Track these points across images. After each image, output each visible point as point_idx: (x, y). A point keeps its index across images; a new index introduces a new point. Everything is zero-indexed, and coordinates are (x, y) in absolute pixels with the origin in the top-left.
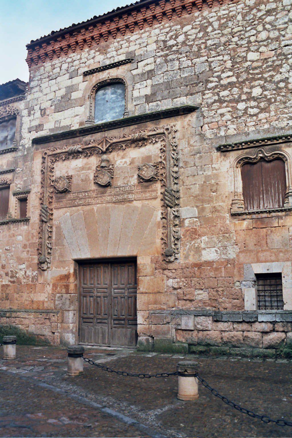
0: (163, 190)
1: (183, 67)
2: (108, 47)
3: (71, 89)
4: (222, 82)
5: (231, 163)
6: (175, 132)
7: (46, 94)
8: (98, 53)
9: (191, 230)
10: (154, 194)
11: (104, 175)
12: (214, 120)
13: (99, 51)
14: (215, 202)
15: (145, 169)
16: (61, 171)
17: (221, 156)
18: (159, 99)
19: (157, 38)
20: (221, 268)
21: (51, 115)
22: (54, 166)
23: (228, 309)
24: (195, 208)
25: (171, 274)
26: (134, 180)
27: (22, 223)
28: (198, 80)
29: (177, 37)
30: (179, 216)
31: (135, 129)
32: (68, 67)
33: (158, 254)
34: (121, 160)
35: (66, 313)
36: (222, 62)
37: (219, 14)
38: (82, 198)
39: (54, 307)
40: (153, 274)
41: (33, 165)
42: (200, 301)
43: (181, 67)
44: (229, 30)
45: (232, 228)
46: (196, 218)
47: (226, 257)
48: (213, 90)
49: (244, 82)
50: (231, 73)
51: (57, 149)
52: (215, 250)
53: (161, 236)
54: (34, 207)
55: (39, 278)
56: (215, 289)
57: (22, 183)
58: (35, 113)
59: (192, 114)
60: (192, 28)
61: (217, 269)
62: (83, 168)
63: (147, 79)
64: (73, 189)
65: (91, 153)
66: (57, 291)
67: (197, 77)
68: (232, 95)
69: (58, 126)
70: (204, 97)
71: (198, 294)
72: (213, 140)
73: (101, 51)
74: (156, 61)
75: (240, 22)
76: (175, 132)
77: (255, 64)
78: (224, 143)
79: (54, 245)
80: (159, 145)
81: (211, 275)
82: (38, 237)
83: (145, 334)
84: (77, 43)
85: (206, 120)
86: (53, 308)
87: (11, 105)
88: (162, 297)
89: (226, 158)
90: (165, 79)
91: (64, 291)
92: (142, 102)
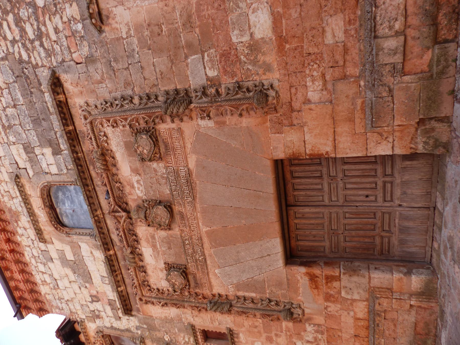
0: (168, 119)
1: (11, 102)
2: (10, 210)
3: (64, 261)
4: (18, 38)
7: (75, 294)
8: (19, 222)
9: (223, 63)
10: (176, 135)
11: (157, 215)
12: (65, 44)
13: (16, 222)
14: (176, 25)
15: (140, 149)
16: (161, 279)
17: (108, 25)
18: (54, 134)
21: (97, 288)
24: (189, 60)
25: (299, 95)
27: (236, 340)
28: (21, 76)
30: (204, 88)
31: (94, 168)
32: (41, 263)
33: (266, 121)
34: (136, 189)
38: (193, 249)
39: (364, 301)
41: (158, 318)
42: (346, 32)
43: (12, 103)
46: (203, 59)
48: (29, 50)
52: (253, 13)
53: (235, 118)
54: (212, 321)
55: (317, 322)
57: (182, 335)
58: (97, 310)
59: (63, 81)
62: (154, 247)
63: (35, 153)
64: (182, 261)
65: (133, 235)
66: (336, 296)
67: (18, 79)
68: (29, 18)
71: (334, 36)
72: (91, 42)
74: (13, 142)
76: (88, 105)
79: (264, 296)
80: (109, 130)
81: (296, 15)
82: (255, 320)
83: (412, 139)
86: (365, 303)
87: (93, 340)
88: (340, 107)
89: (112, 15)
90: (29, 127)
91: (336, 284)
92: (62, 159)
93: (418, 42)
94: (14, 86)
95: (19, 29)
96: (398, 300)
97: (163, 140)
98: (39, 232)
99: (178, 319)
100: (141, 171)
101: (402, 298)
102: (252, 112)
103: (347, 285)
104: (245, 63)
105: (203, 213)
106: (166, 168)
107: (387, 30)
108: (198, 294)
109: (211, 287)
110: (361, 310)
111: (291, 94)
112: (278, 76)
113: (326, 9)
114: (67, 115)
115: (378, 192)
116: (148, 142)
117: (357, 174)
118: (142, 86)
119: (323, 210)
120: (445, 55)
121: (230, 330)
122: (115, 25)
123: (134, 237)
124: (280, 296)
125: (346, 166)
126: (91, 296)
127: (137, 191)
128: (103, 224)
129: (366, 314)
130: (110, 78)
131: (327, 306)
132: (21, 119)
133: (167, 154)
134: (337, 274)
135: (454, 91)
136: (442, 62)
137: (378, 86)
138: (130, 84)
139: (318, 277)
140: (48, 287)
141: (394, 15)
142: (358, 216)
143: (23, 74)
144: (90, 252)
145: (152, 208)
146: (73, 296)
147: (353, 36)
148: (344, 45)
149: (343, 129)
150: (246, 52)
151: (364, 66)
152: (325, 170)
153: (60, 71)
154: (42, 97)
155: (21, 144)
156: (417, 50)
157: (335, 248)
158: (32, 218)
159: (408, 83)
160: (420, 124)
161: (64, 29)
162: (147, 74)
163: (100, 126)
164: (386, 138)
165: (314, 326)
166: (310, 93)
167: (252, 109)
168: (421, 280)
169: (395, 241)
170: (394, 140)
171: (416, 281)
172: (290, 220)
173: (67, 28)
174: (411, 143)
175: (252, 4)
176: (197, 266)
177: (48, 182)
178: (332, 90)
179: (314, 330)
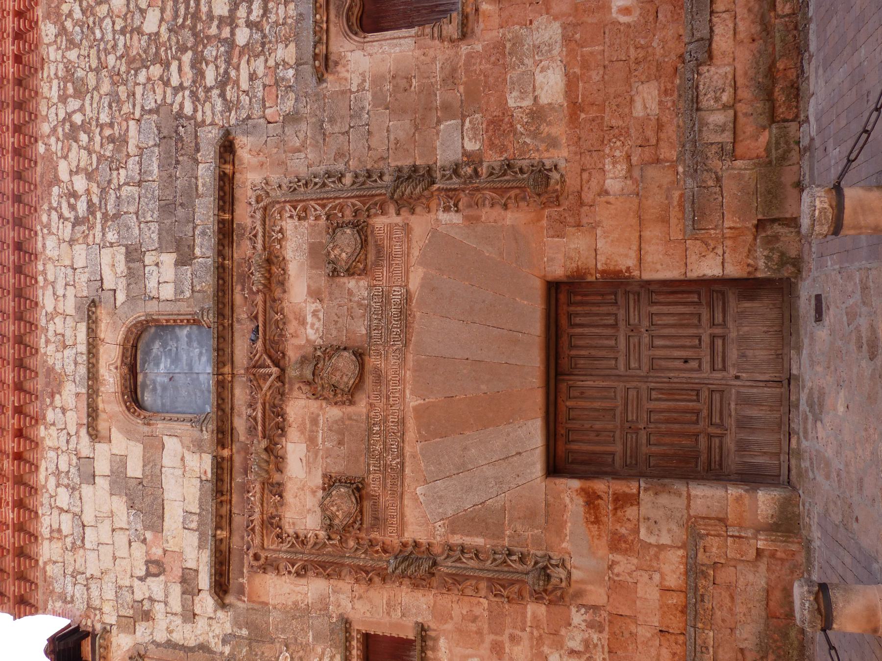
0: (392, 209)
2: (50, 370)
3: (119, 479)
5: (354, 47)
6: (267, 183)
7: (115, 558)
8: (57, 397)
9: (490, 133)
10: (399, 234)
12: (260, 95)
13: (52, 396)
14: (433, 80)
17: (333, 73)
19: (64, 241)
20: (582, 56)
21: (167, 541)
22: (291, 532)
23: (681, 32)
24: (442, 126)
25: (594, 183)
26: (357, 286)
28: (171, 138)
29: (74, 195)
31: (243, 290)
34: (308, 327)
35: (699, 507)
36: (149, 86)
37: (55, 100)
39: (679, 548)
40: (593, 227)
42: (660, 103)
43: (138, 178)
44: (91, 76)
45: (495, 35)
46: (463, 125)
47: (558, 45)
48: (198, 100)
49: (195, 35)
50: (174, 65)
51: (252, 521)
52: (541, 72)
53: (498, 211)
56: (633, 66)
57: (319, 650)
59: (237, 146)
60: (66, 157)
61: (585, 65)
62: (312, 441)
63: (144, 262)
64: (356, 472)
68: (216, 58)
69: (196, 518)
70: (208, 122)
71: (645, 108)
72: (301, 93)
73: (55, 390)
75: (82, 52)
76: (267, 183)
77: (168, 14)
78: (308, 69)
80: (289, 225)
81: (598, 78)
82: (474, 600)
83: (749, 251)
84: (18, 457)
85: (257, 112)
86: (681, 552)
88: (650, 201)
89: (343, 62)
91: (631, 512)
92: (189, 273)
93: (751, 118)
94: (153, 152)
95: (195, 71)
96: (737, 540)
97: (376, 242)
98: (93, 413)
99: (320, 606)
100: (325, 295)
101: (743, 534)
102: (523, 204)
103: (651, 515)
104: (522, 134)
105: (416, 371)
106: (370, 287)
107: (712, 102)
108: (374, 543)
109: (402, 525)
110: (673, 568)
111: (581, 179)
112: (566, 154)
113: (636, 73)
114: (227, 197)
115: (703, 354)
116: (353, 240)
117: (671, 322)
118: (362, 159)
119: (615, 384)
120: (785, 136)
121: (422, 629)
122: (344, 74)
123: (280, 419)
124: (529, 541)
125: (655, 307)
126: (147, 563)
127: (310, 332)
128: (227, 394)
129: (682, 577)
130: (316, 145)
131: (613, 561)
132: (142, 203)
133: (377, 264)
134: (635, 491)
135: (799, 182)
136: (782, 145)
137: (702, 171)
138: (345, 156)
139: (602, 499)
140: (60, 544)
141: (720, 84)
142: (670, 397)
143: (174, 135)
144: (179, 457)
145: (330, 359)
146: (107, 563)
147: (669, 109)
148: (658, 119)
149: (653, 232)
150: (526, 120)
151: (684, 146)
152: (621, 313)
153: (238, 131)
154: (193, 170)
155: (123, 246)
156: (750, 129)
157: (631, 457)
158: (90, 383)
159: (740, 169)
160: (760, 230)
161: (266, 75)
162: (374, 142)
163: (278, 217)
164: (713, 249)
165: (586, 613)
166: (608, 182)
167: (524, 199)
168: (773, 499)
169: (730, 443)
170: (724, 253)
171: (765, 502)
172: (560, 400)
173: (270, 74)
174: (748, 257)
175: (541, 61)
176: (385, 479)
177: (147, 315)
178: (639, 178)
179: (584, 621)
